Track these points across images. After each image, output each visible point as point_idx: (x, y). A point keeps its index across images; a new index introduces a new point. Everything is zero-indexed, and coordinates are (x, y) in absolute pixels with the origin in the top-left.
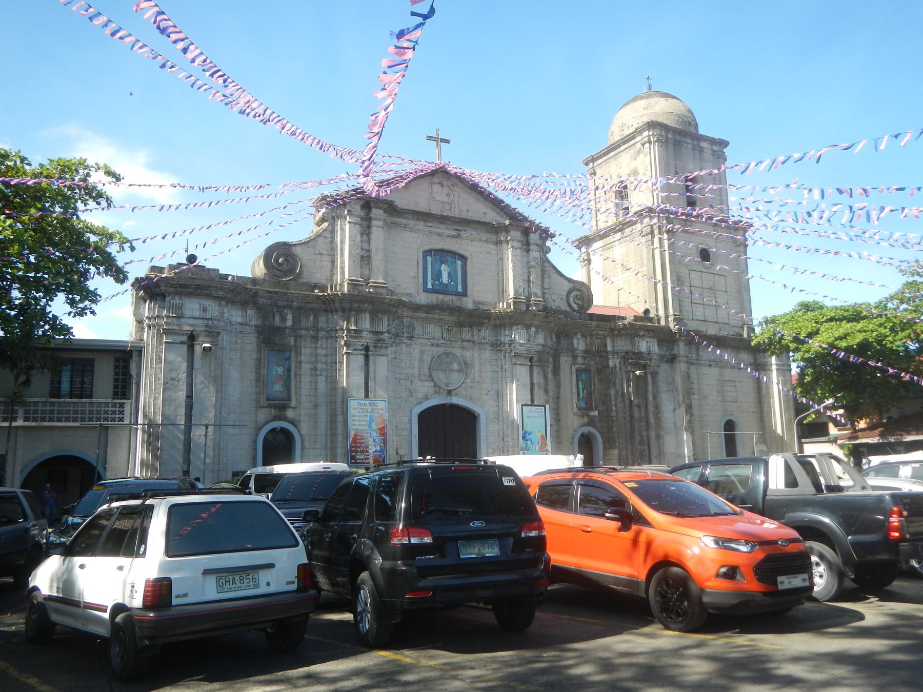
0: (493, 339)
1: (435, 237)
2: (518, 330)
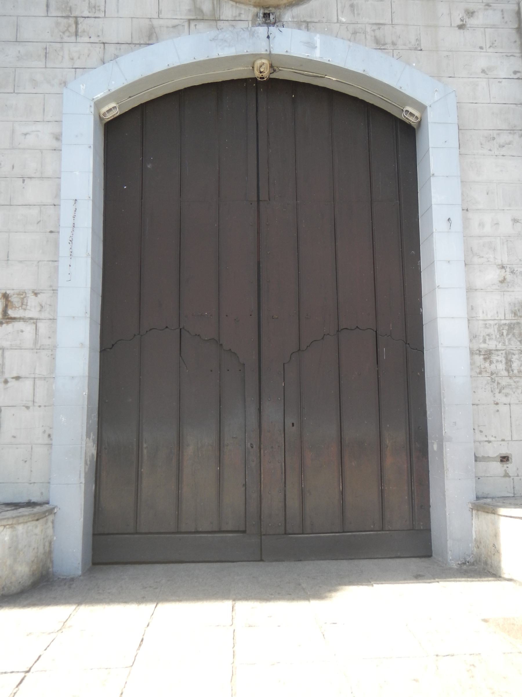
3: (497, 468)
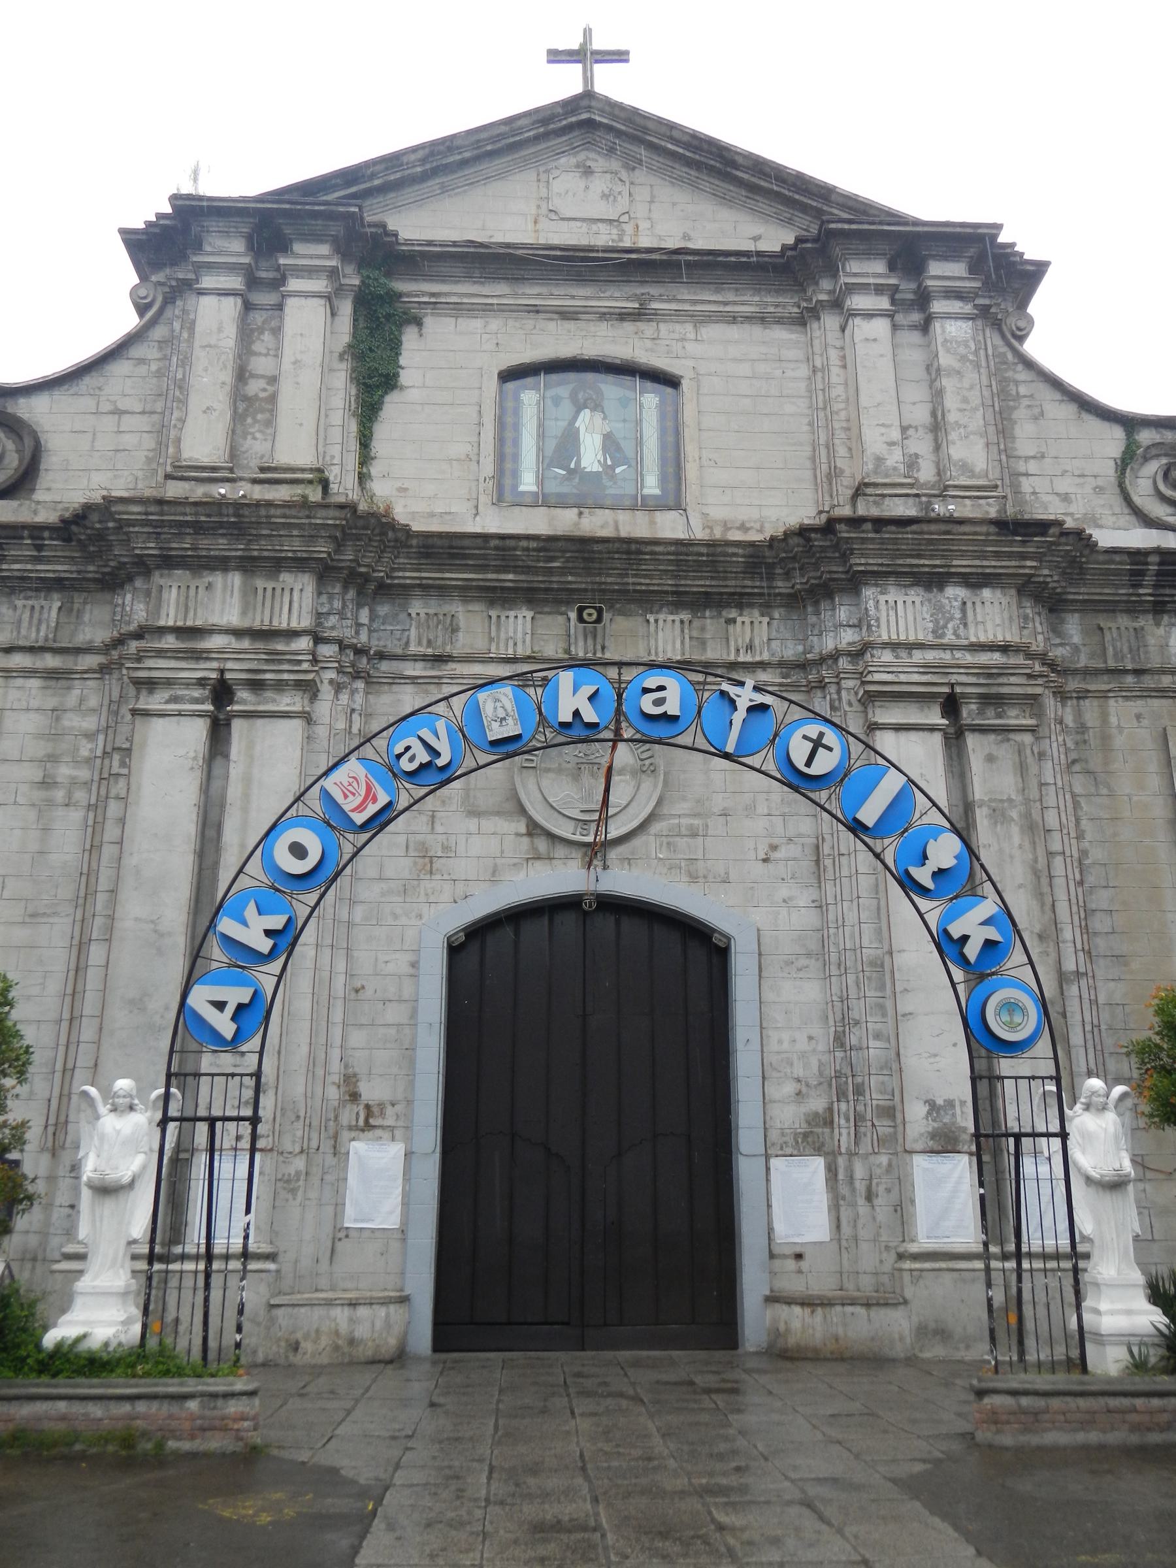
0: (791, 651)
1: (552, 325)
2: (882, 599)
3: (791, 1264)
